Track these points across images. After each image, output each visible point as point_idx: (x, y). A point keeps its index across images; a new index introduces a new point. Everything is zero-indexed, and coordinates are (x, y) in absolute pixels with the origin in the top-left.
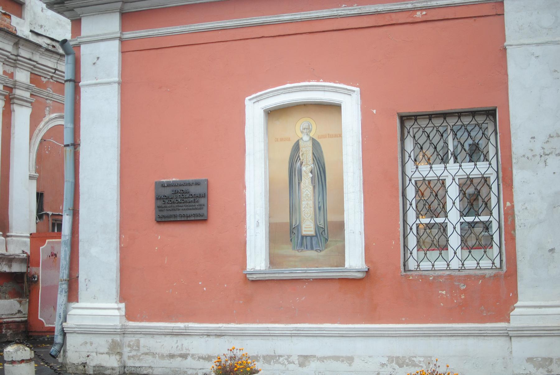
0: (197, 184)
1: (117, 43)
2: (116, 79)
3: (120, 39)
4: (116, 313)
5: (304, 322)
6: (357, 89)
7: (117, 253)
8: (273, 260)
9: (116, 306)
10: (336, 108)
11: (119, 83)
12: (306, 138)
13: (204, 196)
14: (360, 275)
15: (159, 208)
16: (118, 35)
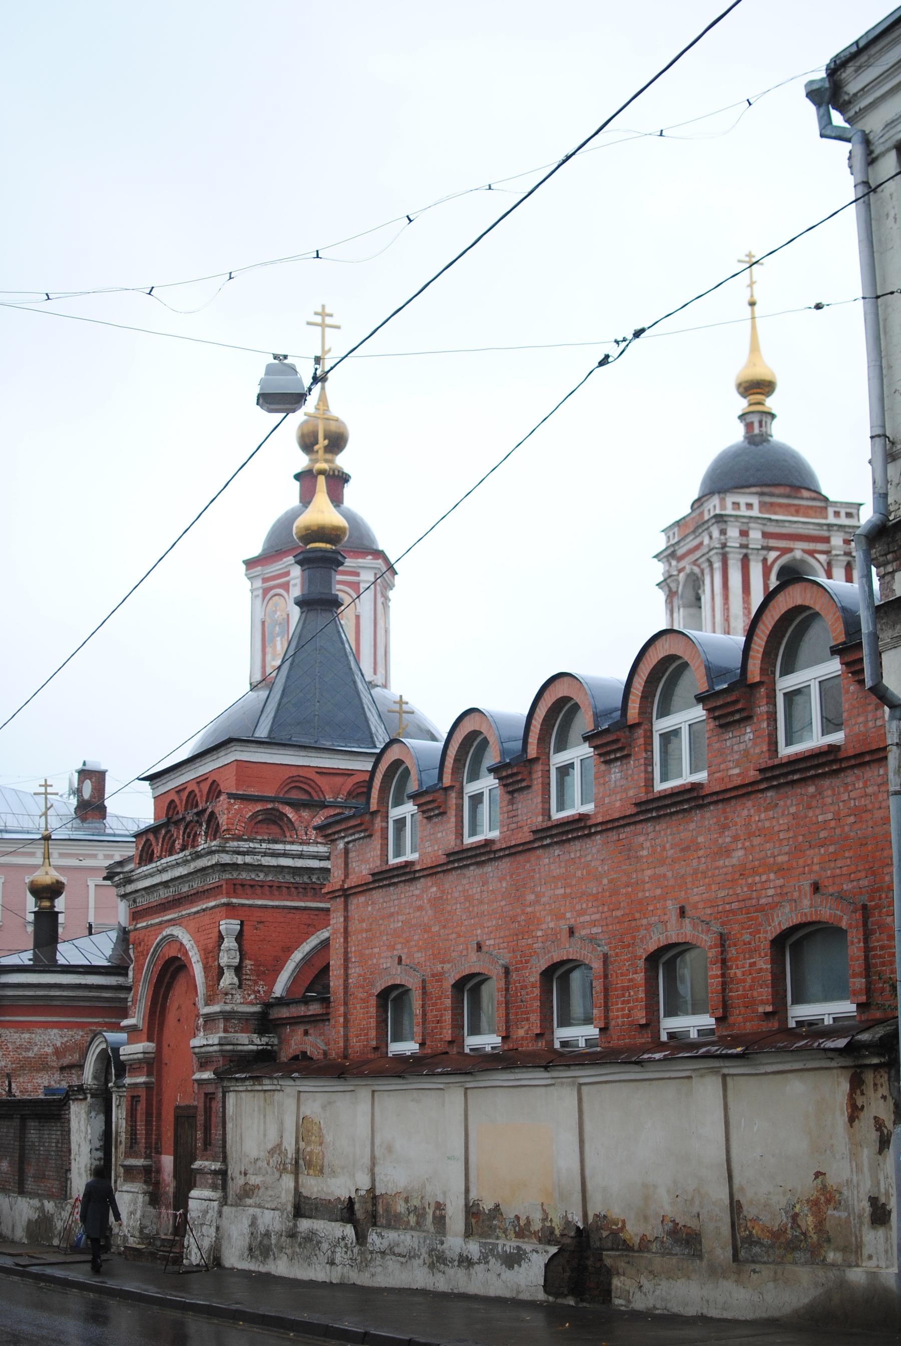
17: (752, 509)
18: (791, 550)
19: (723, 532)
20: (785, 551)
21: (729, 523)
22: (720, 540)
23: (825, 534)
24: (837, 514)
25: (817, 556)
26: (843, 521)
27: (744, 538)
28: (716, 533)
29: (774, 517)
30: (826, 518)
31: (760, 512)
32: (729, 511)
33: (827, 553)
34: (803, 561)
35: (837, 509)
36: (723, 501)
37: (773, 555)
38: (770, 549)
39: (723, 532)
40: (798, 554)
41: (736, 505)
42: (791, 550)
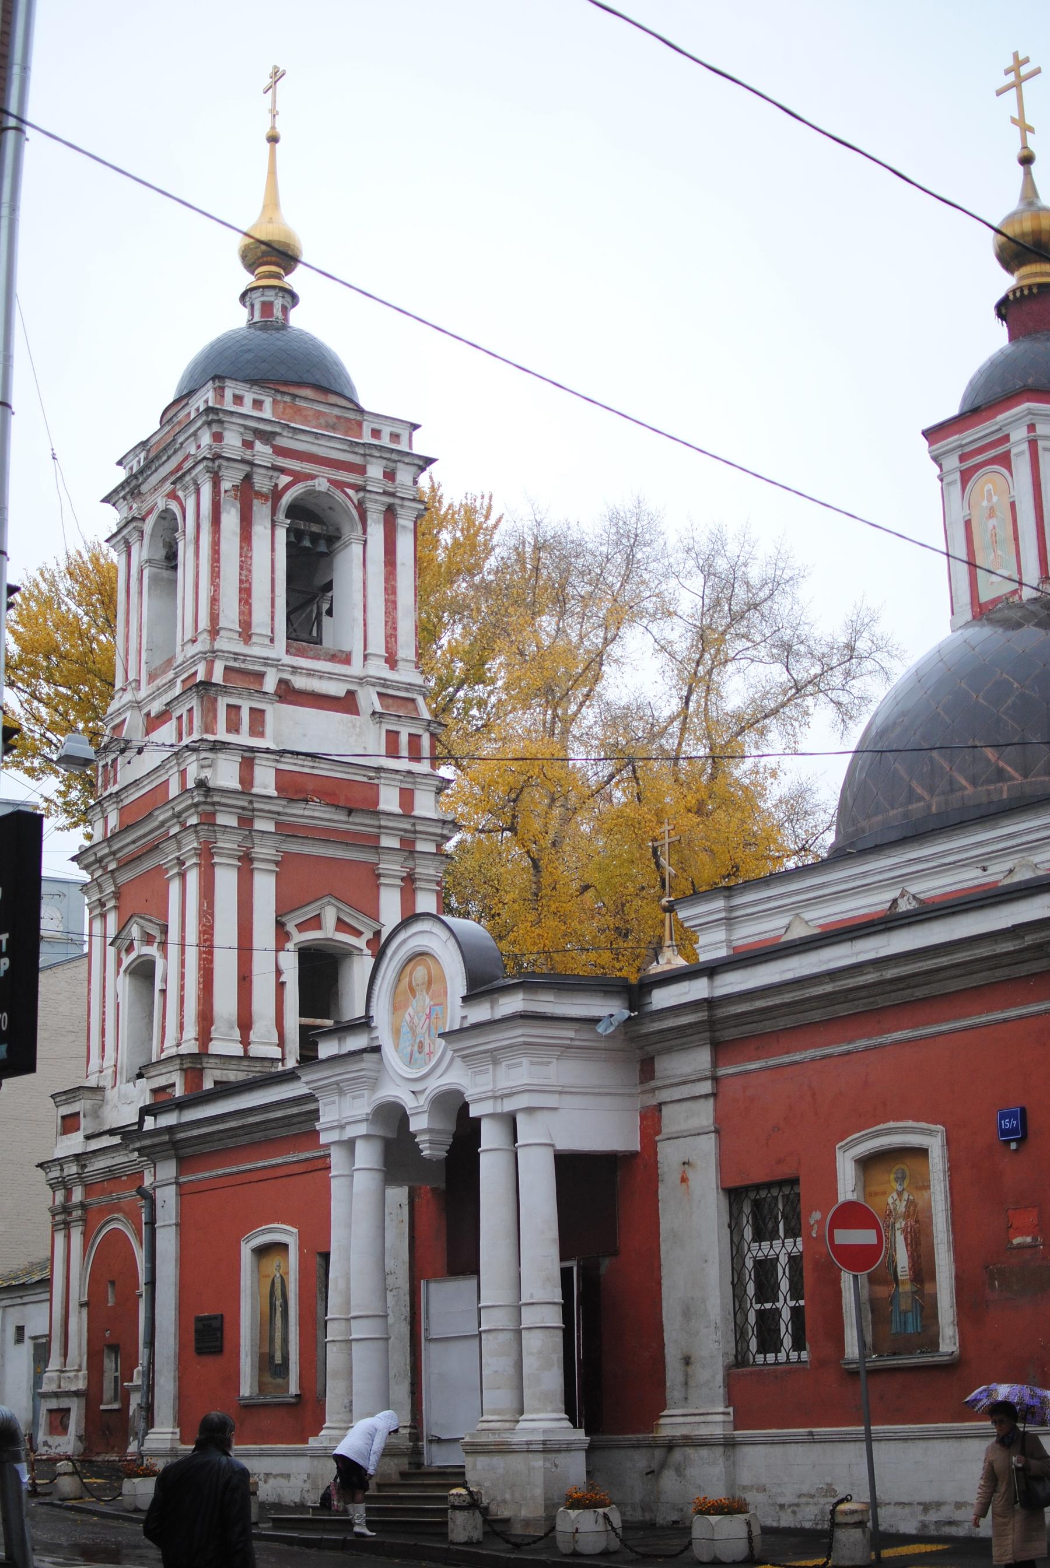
0: (215, 1318)
1: (174, 1186)
2: (174, 1221)
3: (177, 1183)
4: (169, 1436)
5: (268, 1444)
6: (295, 1230)
7: (175, 1382)
8: (262, 1387)
9: (171, 1430)
10: (283, 1247)
11: (176, 1225)
12: (278, 1275)
13: (221, 1329)
14: (293, 1400)
15: (197, 1341)
16: (174, 1180)
17: (241, 404)
18: (313, 477)
19: (218, 437)
20: (298, 477)
21: (226, 425)
22: (210, 447)
23: (357, 460)
24: (376, 433)
25: (348, 490)
26: (385, 441)
27: (249, 452)
28: (206, 439)
29: (293, 425)
30: (360, 436)
31: (274, 414)
32: (229, 405)
33: (359, 488)
34: (326, 494)
35: (376, 426)
36: (220, 391)
37: (284, 480)
38: (283, 471)
39: (218, 437)
40: (322, 485)
41: (238, 399)
42: (313, 477)
